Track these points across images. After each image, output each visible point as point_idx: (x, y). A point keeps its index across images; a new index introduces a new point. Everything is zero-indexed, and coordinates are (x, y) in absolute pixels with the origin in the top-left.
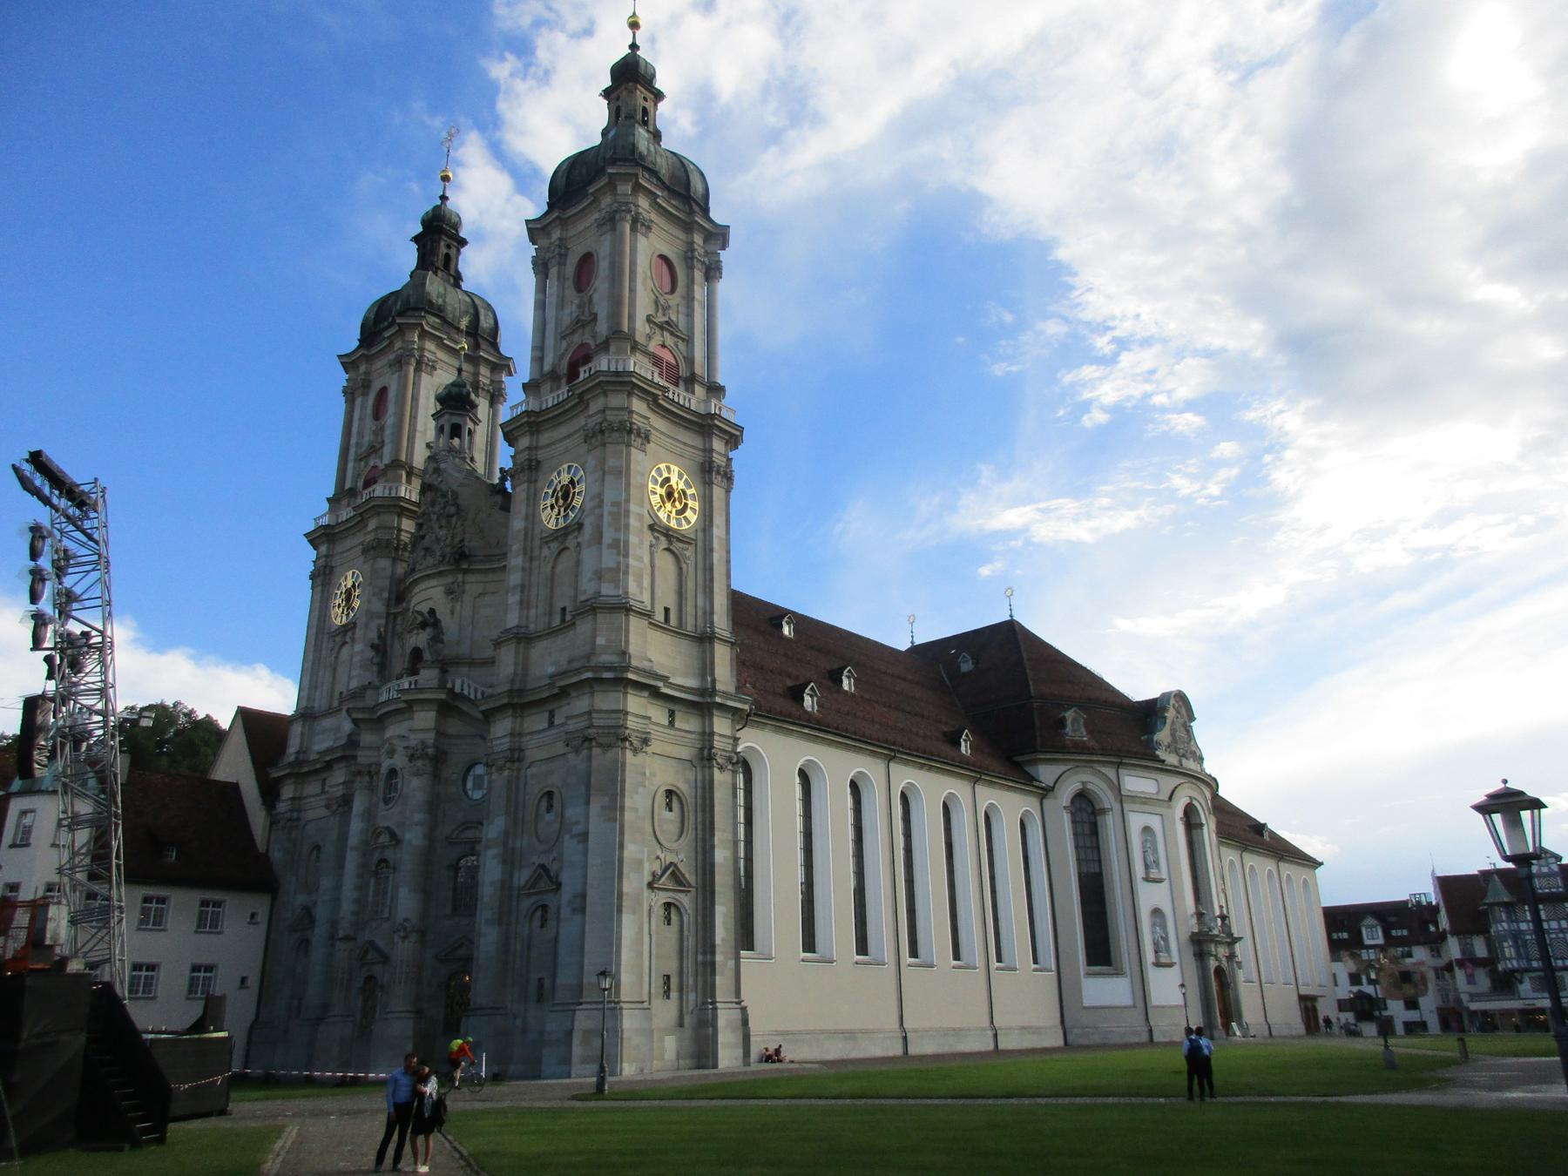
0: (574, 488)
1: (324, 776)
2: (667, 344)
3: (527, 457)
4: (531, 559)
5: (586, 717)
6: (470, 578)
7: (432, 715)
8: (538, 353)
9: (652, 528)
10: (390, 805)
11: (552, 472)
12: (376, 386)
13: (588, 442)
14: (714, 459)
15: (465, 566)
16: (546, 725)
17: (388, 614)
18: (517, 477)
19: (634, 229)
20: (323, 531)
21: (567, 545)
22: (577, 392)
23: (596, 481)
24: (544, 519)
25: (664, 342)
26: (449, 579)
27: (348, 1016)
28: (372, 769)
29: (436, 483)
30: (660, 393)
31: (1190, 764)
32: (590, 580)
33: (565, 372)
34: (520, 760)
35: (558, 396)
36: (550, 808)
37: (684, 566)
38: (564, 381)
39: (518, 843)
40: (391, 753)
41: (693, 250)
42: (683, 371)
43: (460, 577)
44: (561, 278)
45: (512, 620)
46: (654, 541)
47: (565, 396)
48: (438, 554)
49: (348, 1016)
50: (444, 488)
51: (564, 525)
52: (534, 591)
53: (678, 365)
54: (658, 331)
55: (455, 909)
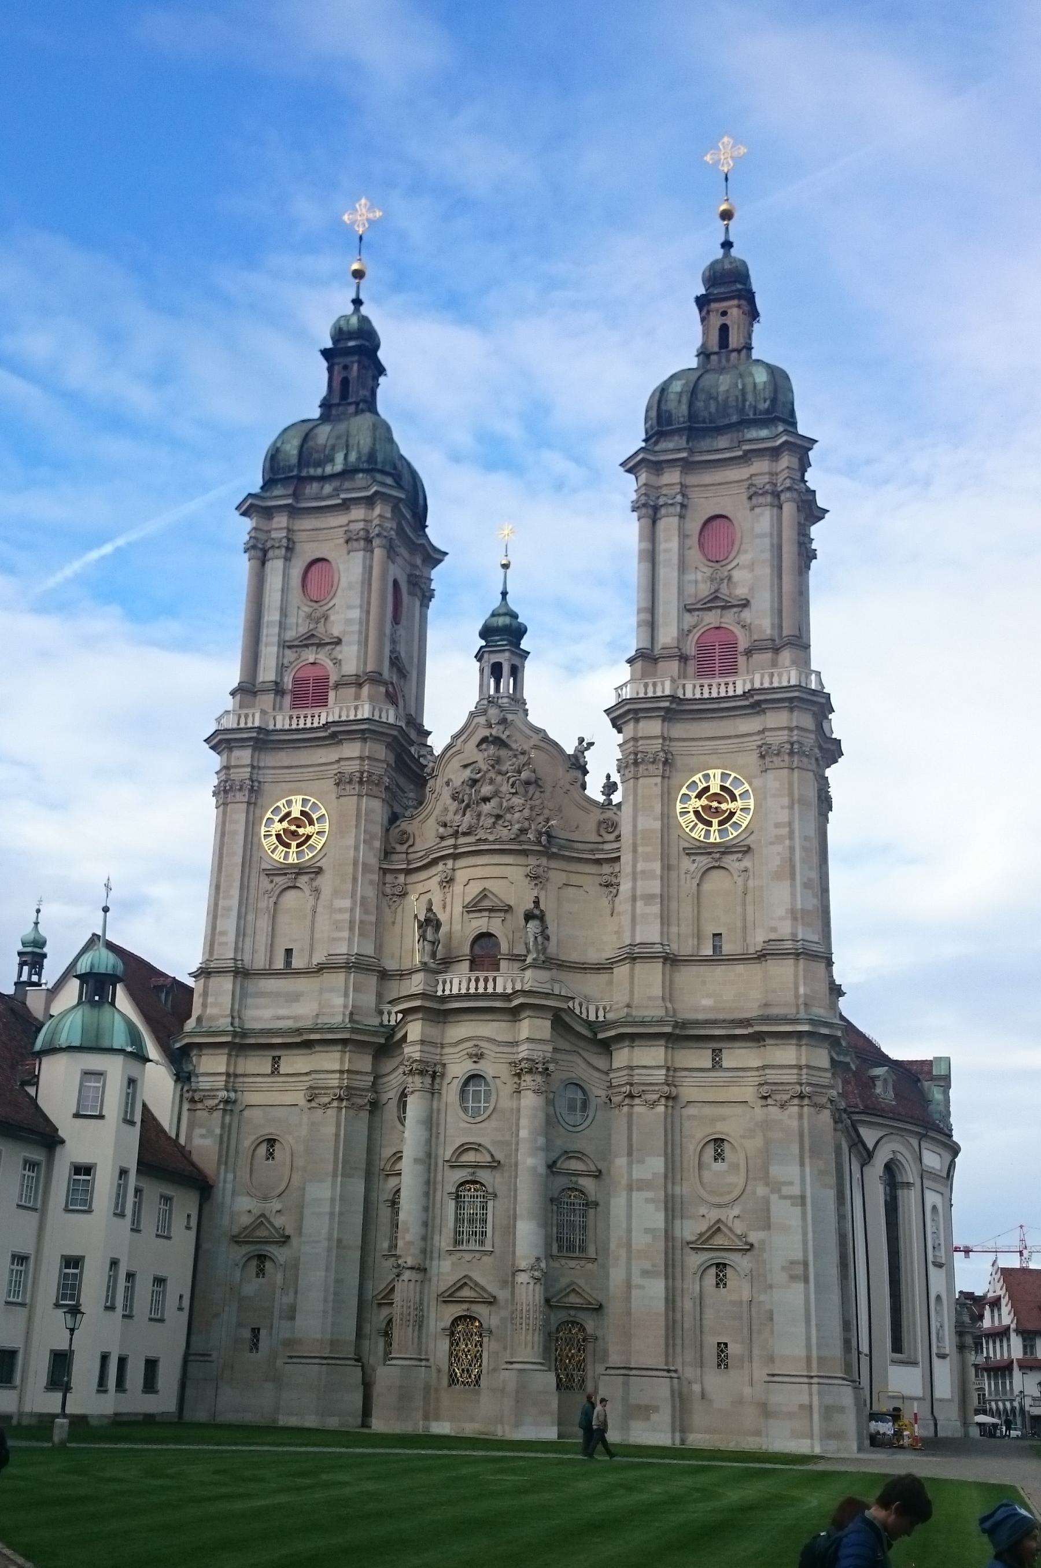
1: (277, 1053)
4: (667, 867)
6: (553, 864)
7: (548, 1023)
8: (648, 617)
10: (479, 1119)
11: (694, 771)
12: (308, 551)
15: (555, 850)
17: (380, 868)
20: (254, 735)
23: (782, 807)
26: (532, 860)
27: (421, 1360)
28: (439, 1068)
29: (504, 737)
31: (947, 1132)
32: (781, 918)
34: (675, 1098)
36: (719, 1156)
39: (678, 1190)
40: (478, 1057)
43: (544, 861)
44: (683, 536)
45: (650, 932)
48: (517, 826)
49: (421, 1360)
50: (514, 746)
52: (674, 905)
55: (560, 1248)
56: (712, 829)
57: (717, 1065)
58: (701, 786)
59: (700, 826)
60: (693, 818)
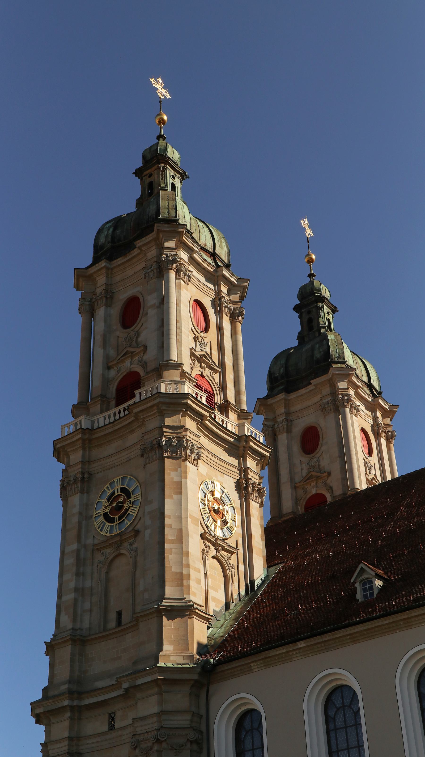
0: (129, 496)
2: (204, 375)
3: (80, 470)
5: (155, 719)
9: (203, 536)
13: (145, 455)
14: (250, 477)
16: (105, 728)
18: (69, 488)
19: (178, 277)
21: (123, 551)
22: (135, 411)
24: (97, 527)
25: (202, 372)
30: (208, 414)
33: (114, 395)
35: (109, 417)
37: (229, 574)
38: (113, 403)
41: (221, 298)
42: (218, 400)
46: (206, 549)
47: (112, 419)
51: (118, 532)
53: (214, 393)
54: (198, 364)
56: (114, 524)
57: (112, 727)
58: (109, 492)
59: (107, 524)
60: (104, 520)
